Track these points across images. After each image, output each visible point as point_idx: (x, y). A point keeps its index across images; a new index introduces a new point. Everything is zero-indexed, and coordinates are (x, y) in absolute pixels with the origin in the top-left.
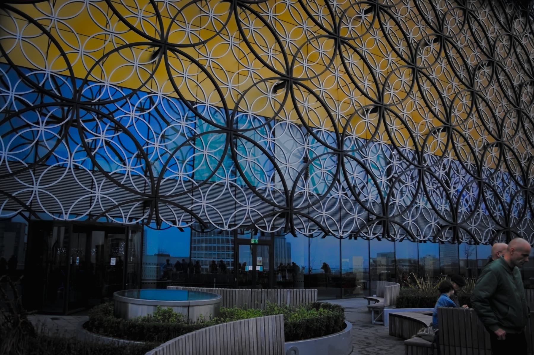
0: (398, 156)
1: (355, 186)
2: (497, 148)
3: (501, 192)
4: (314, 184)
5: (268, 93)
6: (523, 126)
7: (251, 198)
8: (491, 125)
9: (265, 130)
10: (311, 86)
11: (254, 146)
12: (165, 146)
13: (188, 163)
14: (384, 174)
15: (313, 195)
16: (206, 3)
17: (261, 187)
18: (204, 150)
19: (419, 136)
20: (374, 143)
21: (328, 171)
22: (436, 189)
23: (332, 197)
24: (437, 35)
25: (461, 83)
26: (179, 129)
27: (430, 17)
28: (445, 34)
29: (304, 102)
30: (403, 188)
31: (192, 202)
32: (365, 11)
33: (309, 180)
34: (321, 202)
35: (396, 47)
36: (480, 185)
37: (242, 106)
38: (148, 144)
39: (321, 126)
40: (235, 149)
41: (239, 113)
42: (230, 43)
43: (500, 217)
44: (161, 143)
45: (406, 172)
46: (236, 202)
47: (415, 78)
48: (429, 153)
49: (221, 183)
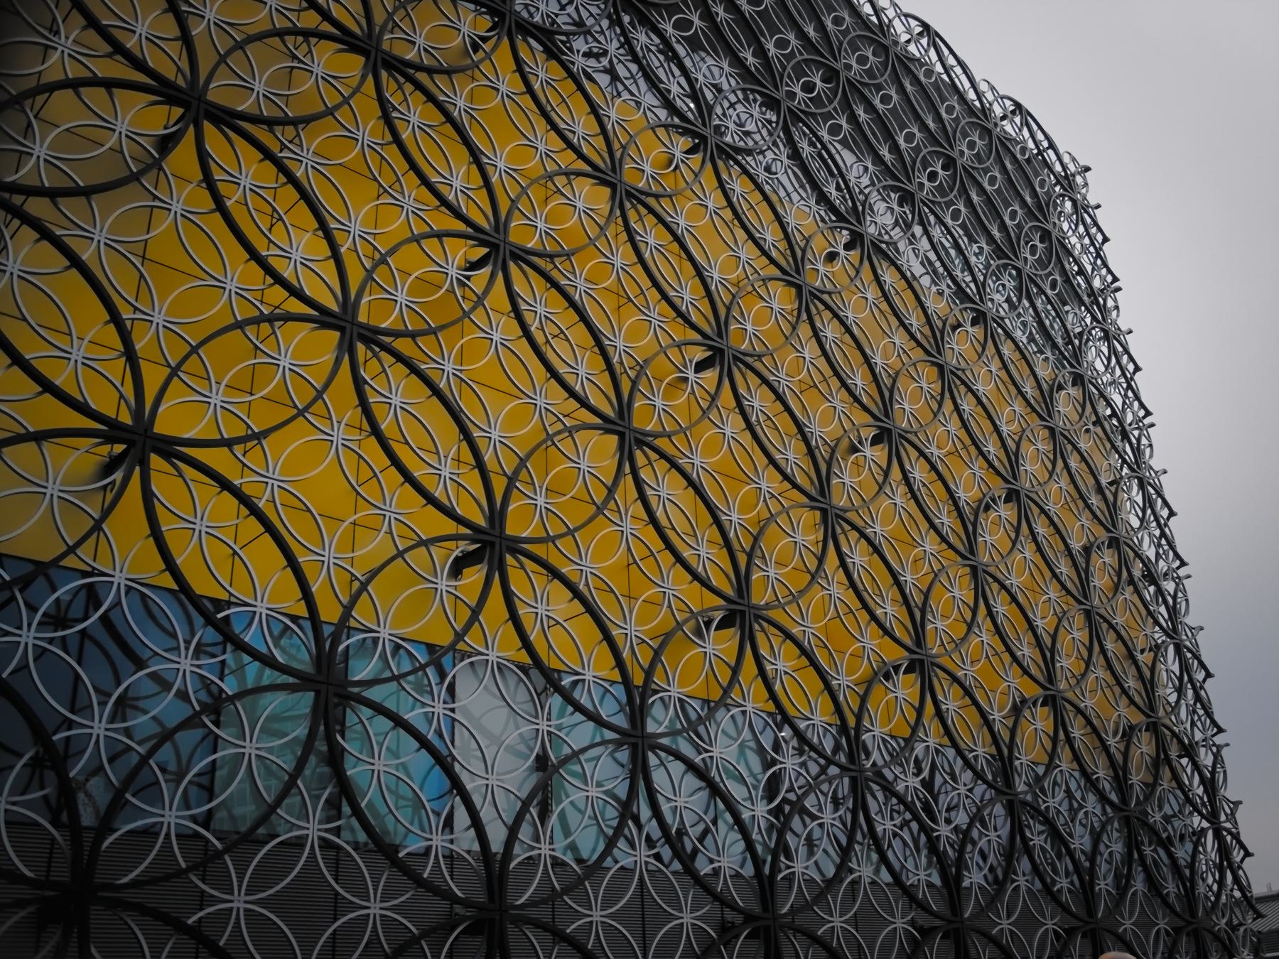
0: (794, 743)
1: (681, 832)
2: (1046, 709)
3: (1066, 824)
4: (567, 833)
5: (437, 578)
6: (1103, 651)
7: (383, 880)
8: (1027, 651)
9: (426, 682)
10: (555, 560)
11: (394, 728)
12: (127, 732)
13: (196, 779)
14: (760, 794)
15: (564, 864)
16: (271, 331)
17: (415, 845)
18: (245, 741)
19: (848, 686)
20: (729, 711)
21: (605, 792)
22: (901, 830)
23: (618, 866)
24: (879, 427)
25: (944, 546)
26: (171, 680)
27: (860, 380)
28: (898, 424)
29: (537, 602)
30: (812, 829)
31: (203, 900)
32: (697, 364)
33: (554, 819)
34: (587, 883)
35: (778, 457)
36: (1011, 808)
37: (361, 615)
38: (70, 724)
39: (584, 668)
40: (339, 738)
41: (352, 632)
42: (335, 439)
43: (1070, 891)
44: (112, 720)
45: (818, 785)
46: (337, 894)
47: (830, 536)
48: (876, 731)
49: (297, 837)
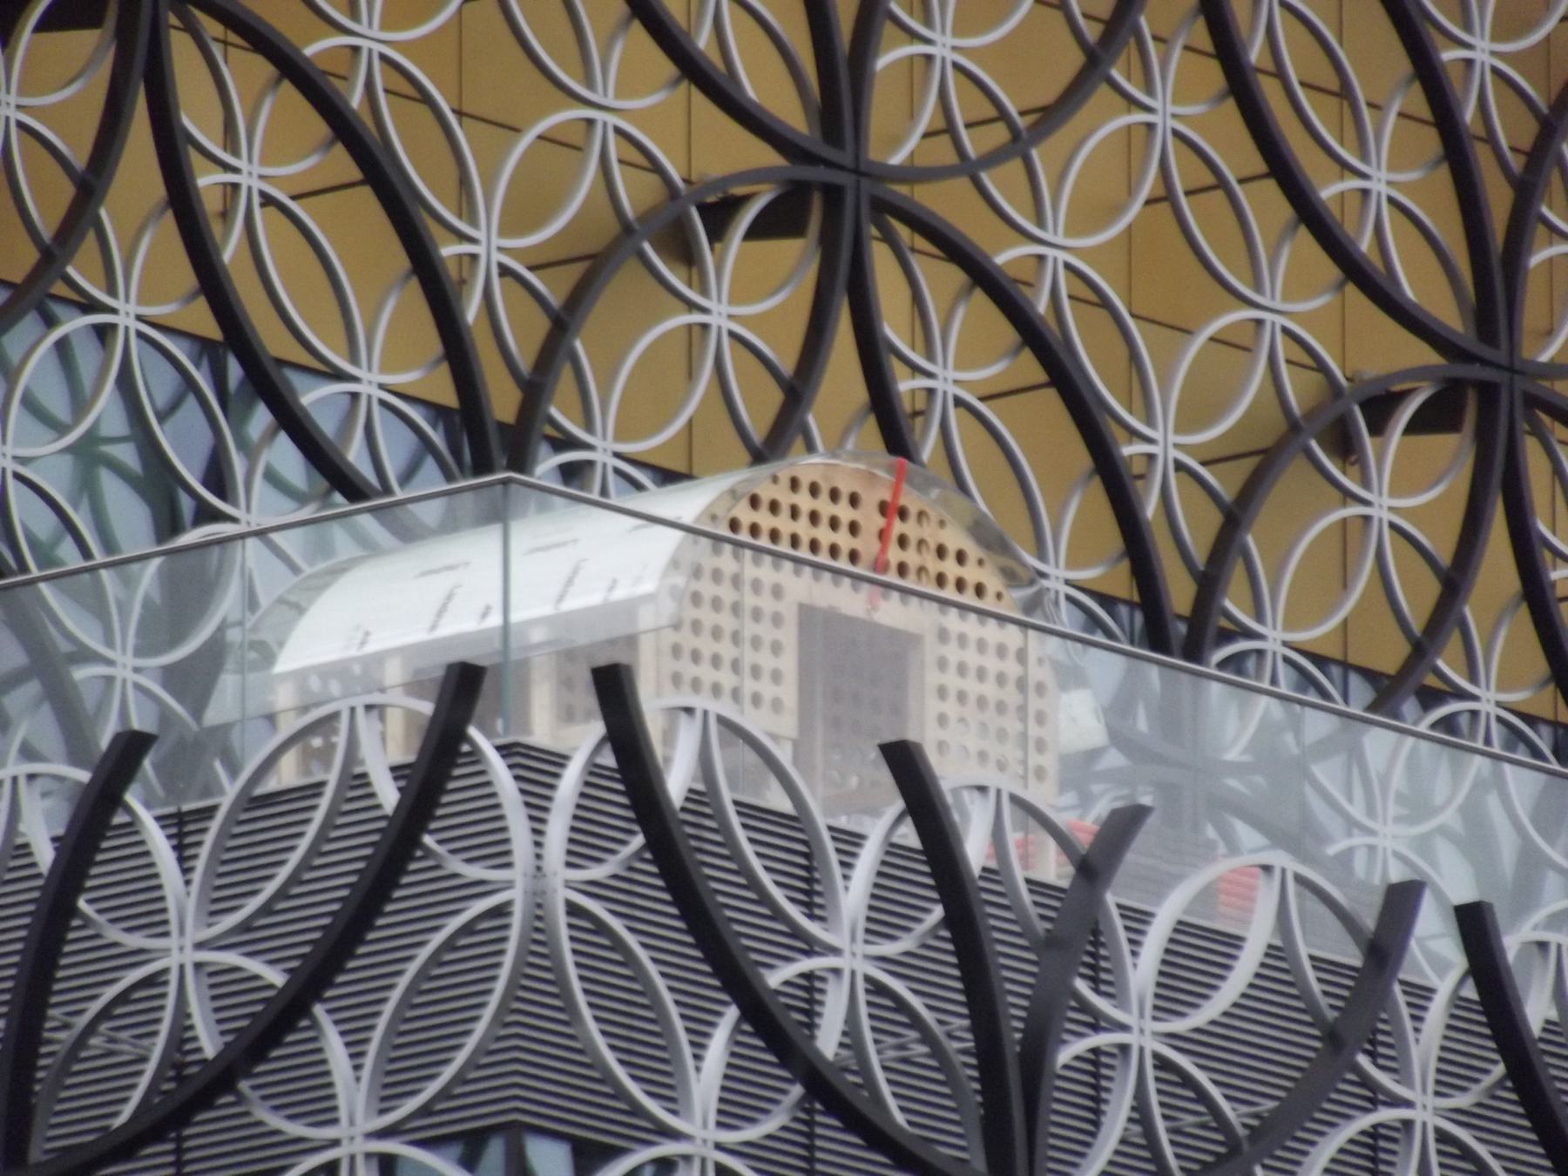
20: (50, 322)
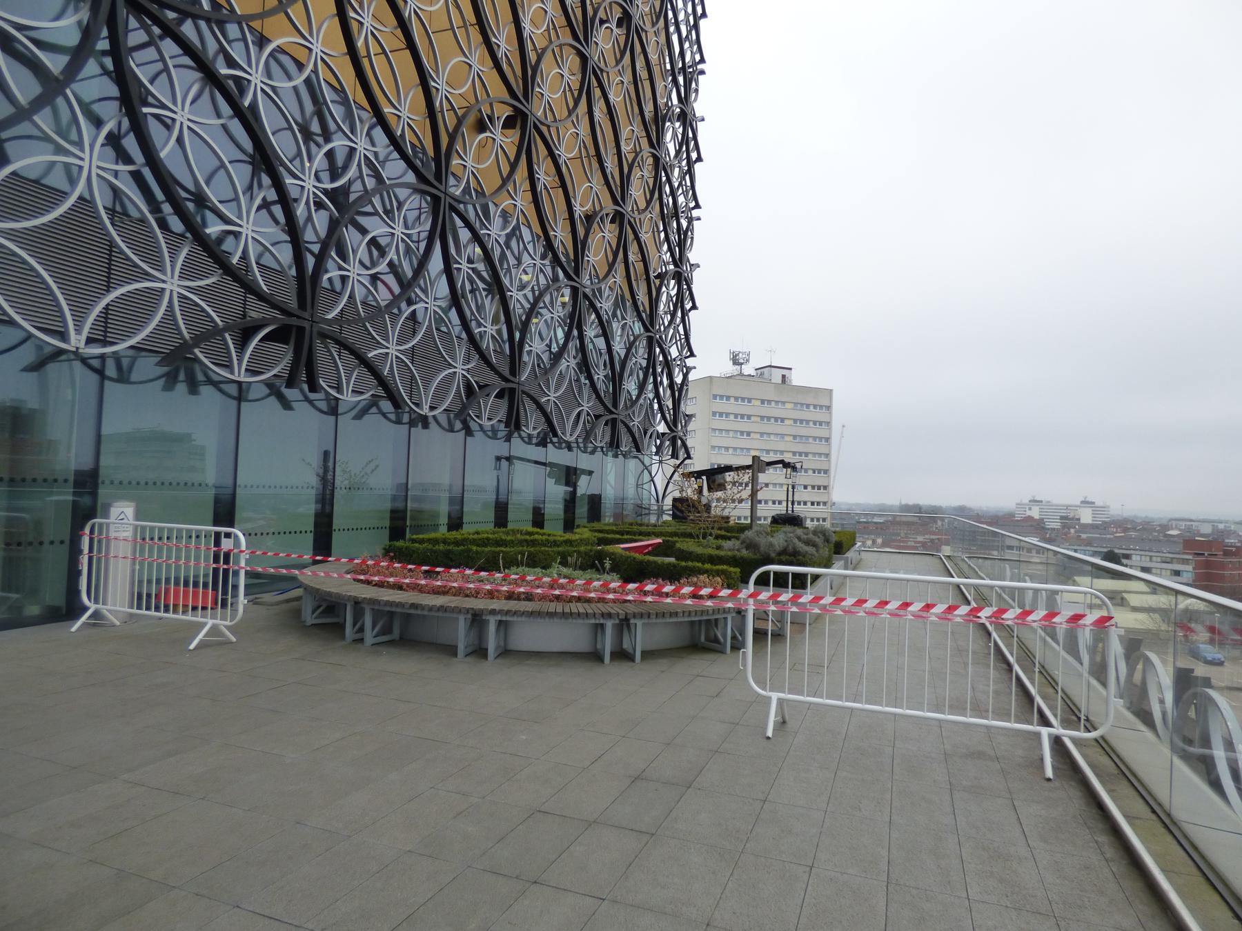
47: (440, 233)
